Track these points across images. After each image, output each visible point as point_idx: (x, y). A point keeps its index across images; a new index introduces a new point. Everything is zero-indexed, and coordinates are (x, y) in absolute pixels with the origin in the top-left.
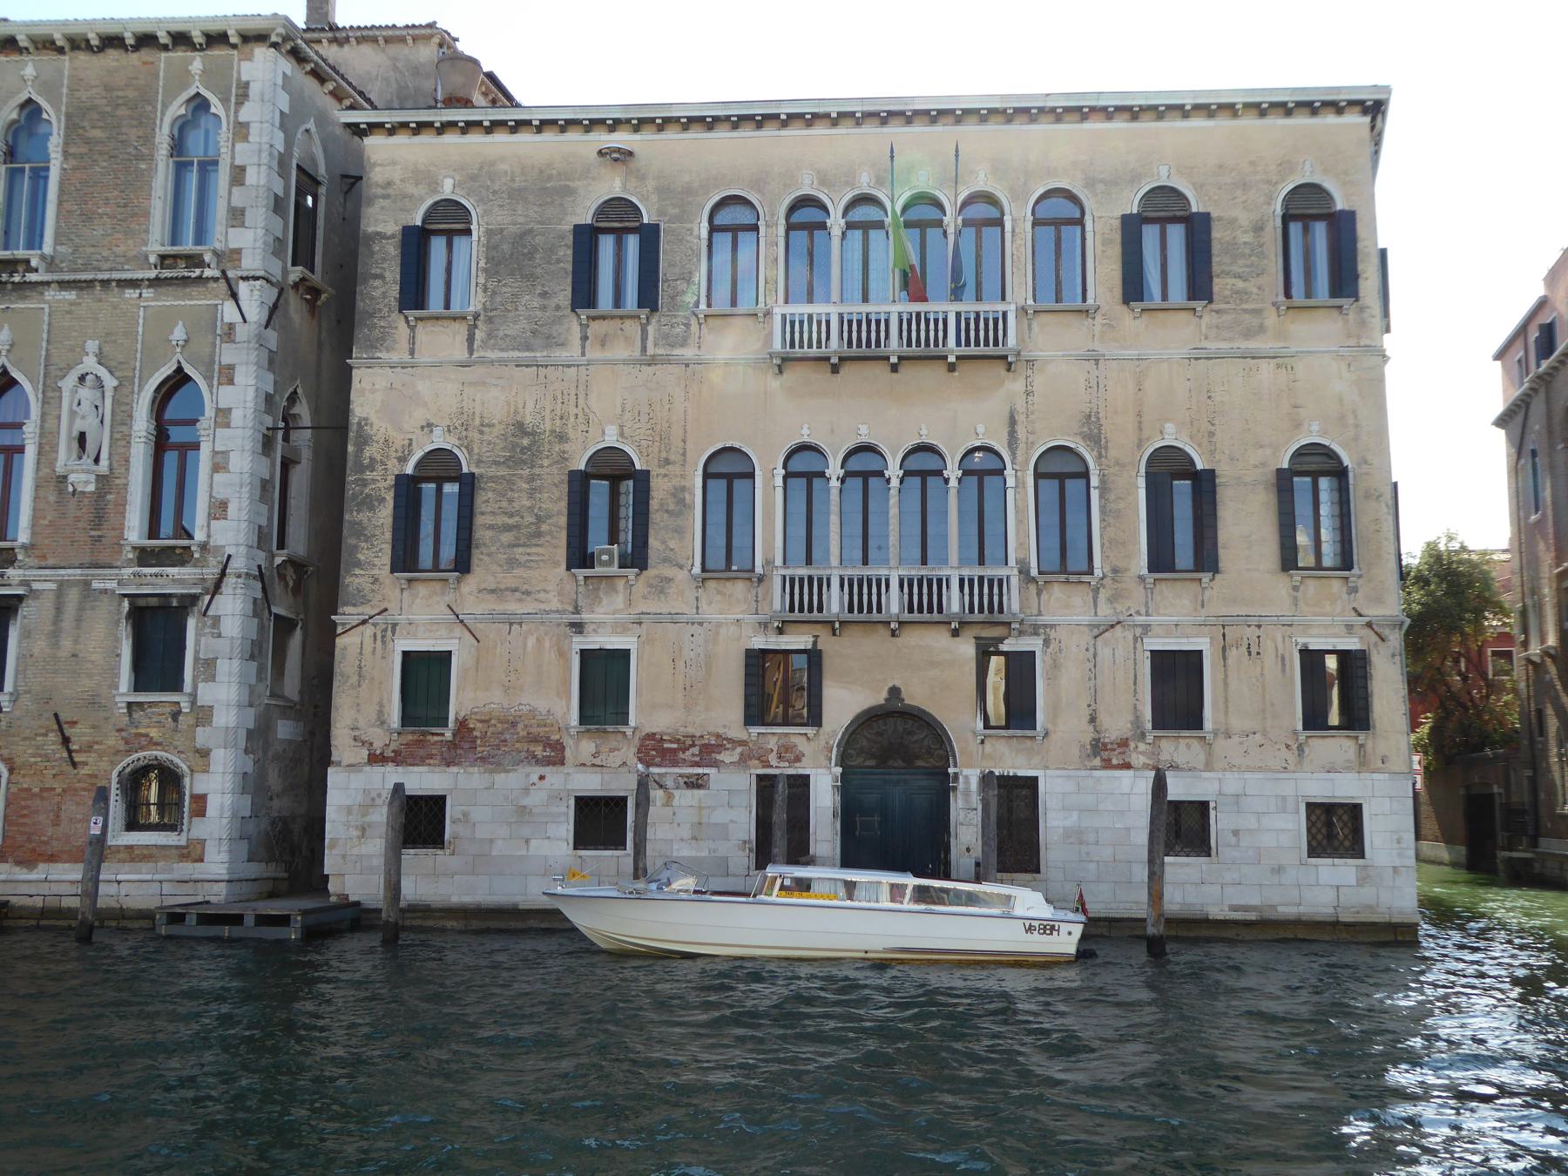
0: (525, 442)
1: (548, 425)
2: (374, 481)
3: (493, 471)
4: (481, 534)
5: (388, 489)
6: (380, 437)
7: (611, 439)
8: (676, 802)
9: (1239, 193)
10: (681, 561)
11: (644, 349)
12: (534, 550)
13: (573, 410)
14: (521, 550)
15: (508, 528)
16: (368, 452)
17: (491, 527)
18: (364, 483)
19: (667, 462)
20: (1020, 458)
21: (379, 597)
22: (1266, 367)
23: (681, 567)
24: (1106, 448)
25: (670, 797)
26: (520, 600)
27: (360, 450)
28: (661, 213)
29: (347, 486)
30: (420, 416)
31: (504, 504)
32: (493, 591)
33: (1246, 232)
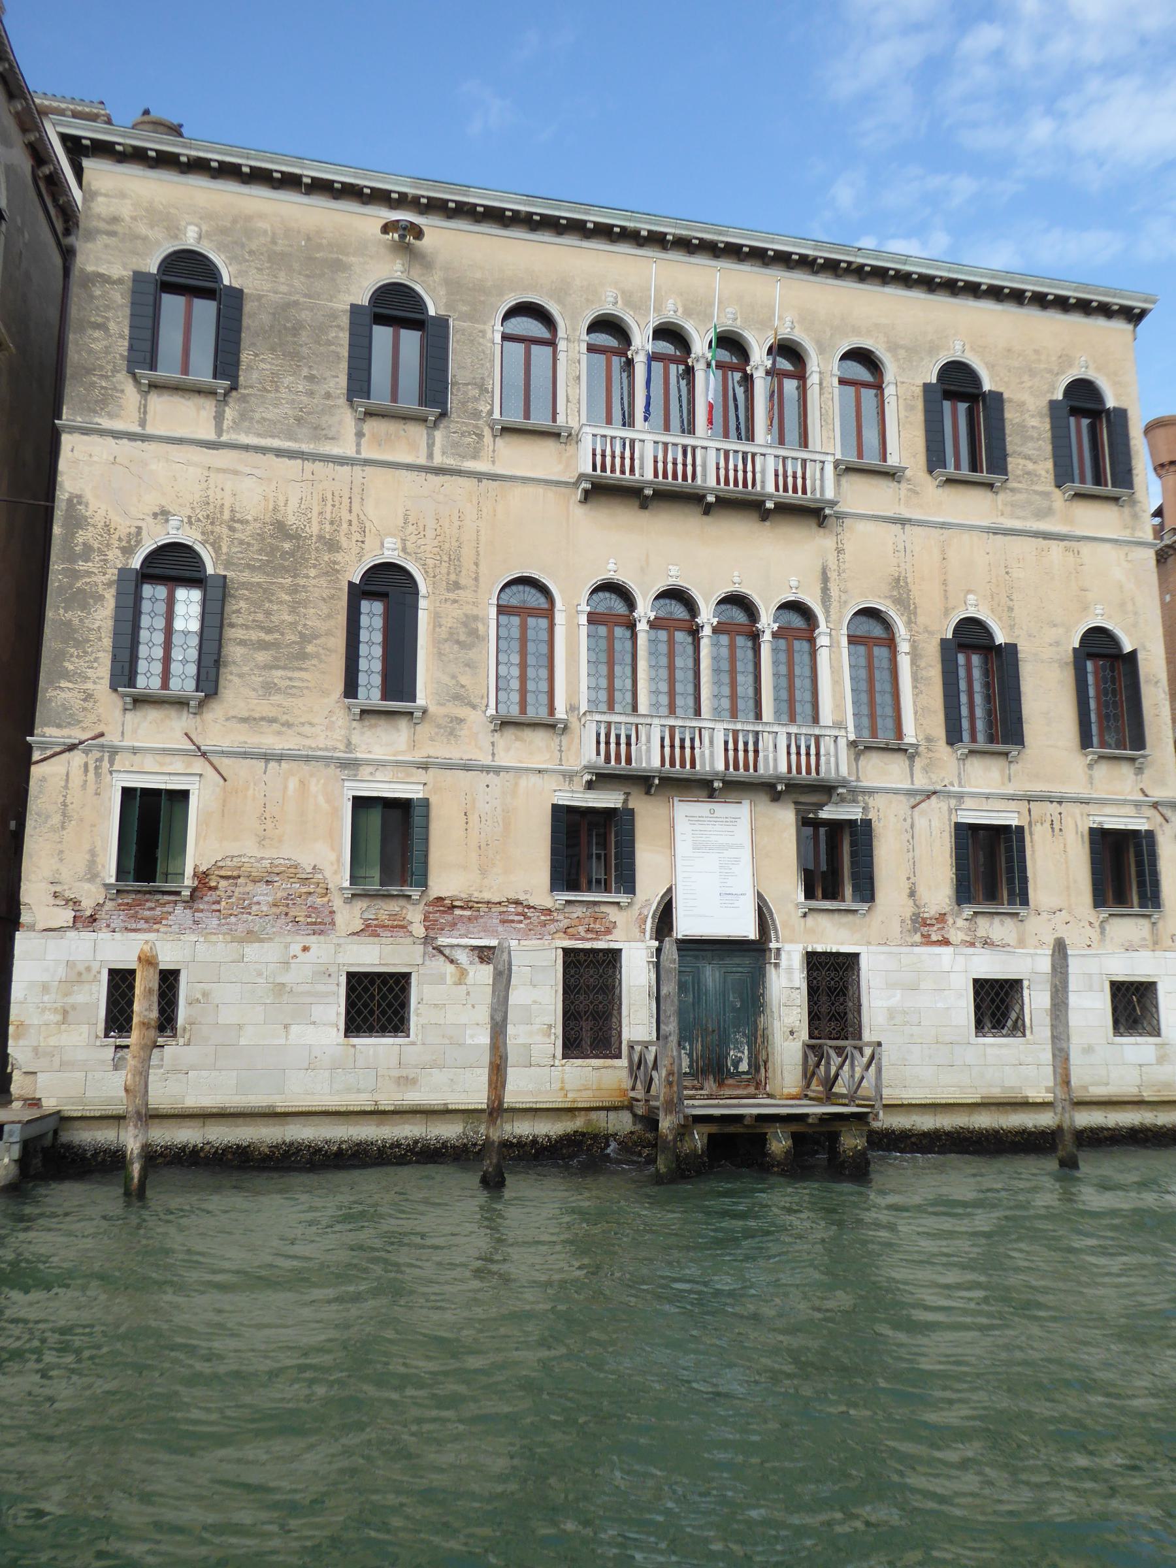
1: (315, 530)
2: (89, 573)
3: (245, 576)
4: (234, 652)
5: (109, 584)
6: (99, 520)
7: (391, 554)
8: (470, 979)
9: (1026, 378)
10: (476, 701)
11: (430, 456)
12: (296, 674)
14: (280, 673)
15: (263, 646)
16: (81, 537)
17: (243, 643)
18: (75, 575)
19: (457, 586)
20: (834, 616)
21: (92, 717)
22: (1056, 547)
23: (474, 707)
24: (915, 614)
25: (463, 973)
26: (279, 733)
27: (70, 536)
28: (448, 306)
29: (51, 577)
30: (152, 501)
31: (260, 617)
32: (244, 720)
33: (1033, 416)
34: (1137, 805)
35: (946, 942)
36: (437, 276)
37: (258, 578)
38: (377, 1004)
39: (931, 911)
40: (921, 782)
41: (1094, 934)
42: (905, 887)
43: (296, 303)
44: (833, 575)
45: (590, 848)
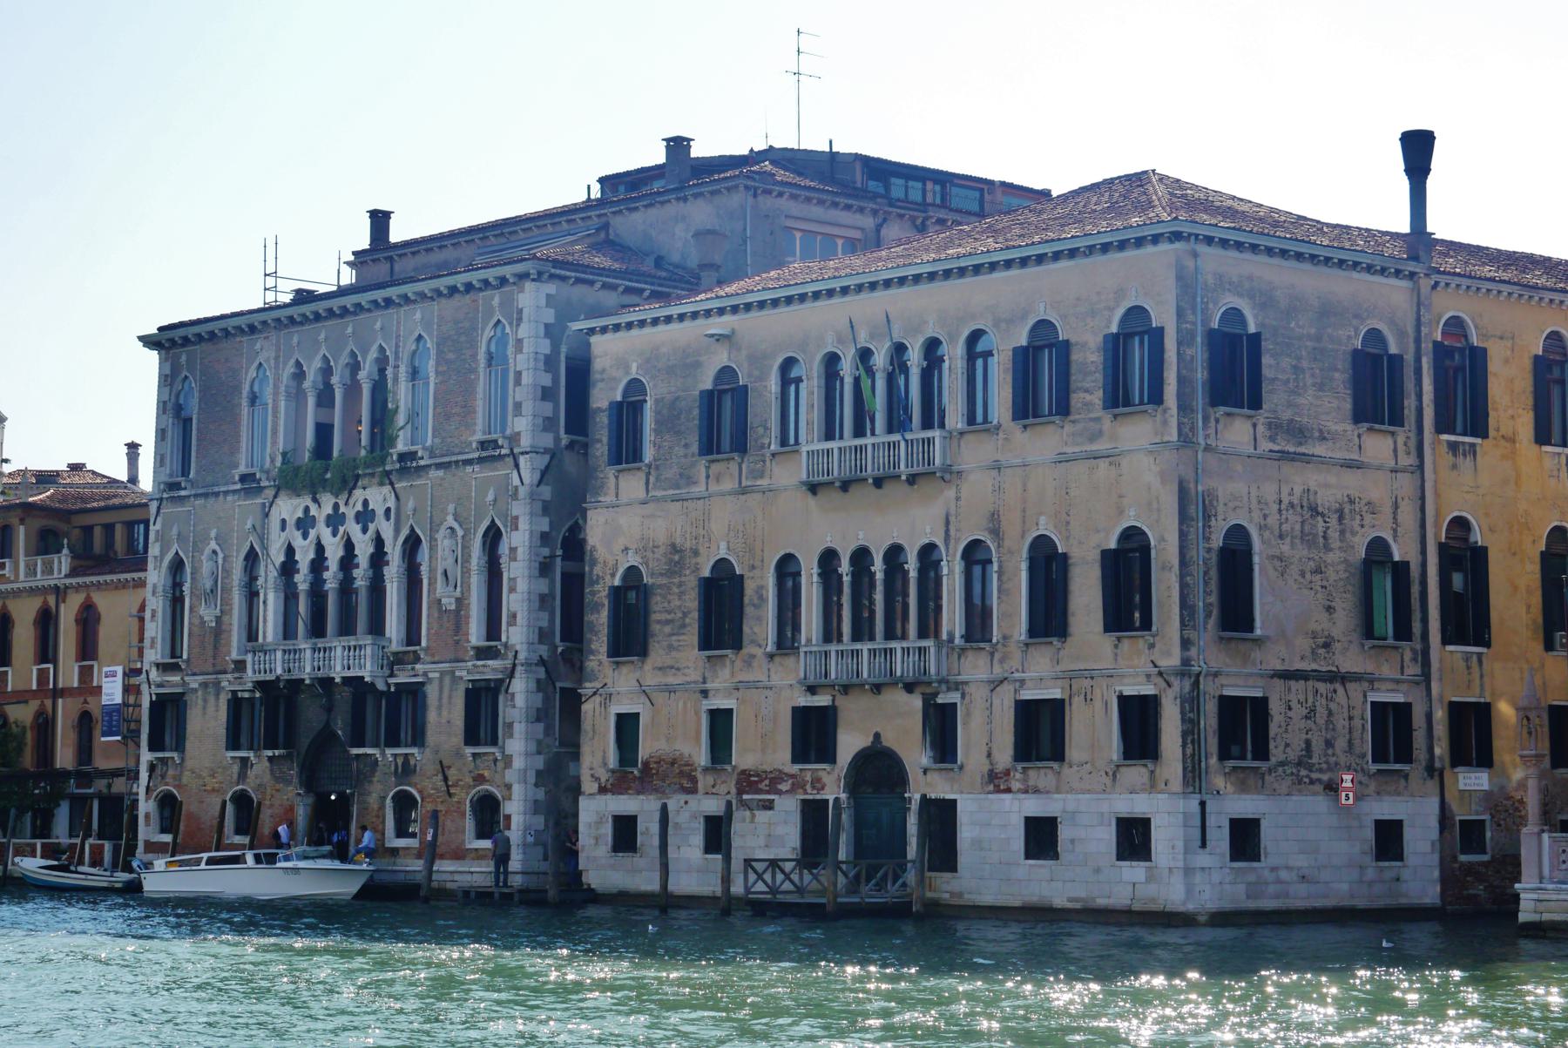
0: (676, 558)
6: (601, 560)
13: (702, 532)
15: (668, 622)
17: (659, 622)
25: (753, 816)
30: (621, 542)
34: (1148, 676)
35: (1009, 790)
36: (744, 353)
37: (664, 581)
38: (717, 834)
39: (1000, 767)
40: (997, 670)
41: (1108, 781)
42: (985, 749)
43: (677, 398)
44: (952, 519)
45: (813, 733)
